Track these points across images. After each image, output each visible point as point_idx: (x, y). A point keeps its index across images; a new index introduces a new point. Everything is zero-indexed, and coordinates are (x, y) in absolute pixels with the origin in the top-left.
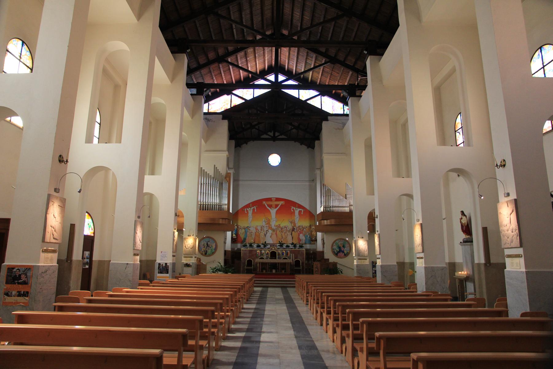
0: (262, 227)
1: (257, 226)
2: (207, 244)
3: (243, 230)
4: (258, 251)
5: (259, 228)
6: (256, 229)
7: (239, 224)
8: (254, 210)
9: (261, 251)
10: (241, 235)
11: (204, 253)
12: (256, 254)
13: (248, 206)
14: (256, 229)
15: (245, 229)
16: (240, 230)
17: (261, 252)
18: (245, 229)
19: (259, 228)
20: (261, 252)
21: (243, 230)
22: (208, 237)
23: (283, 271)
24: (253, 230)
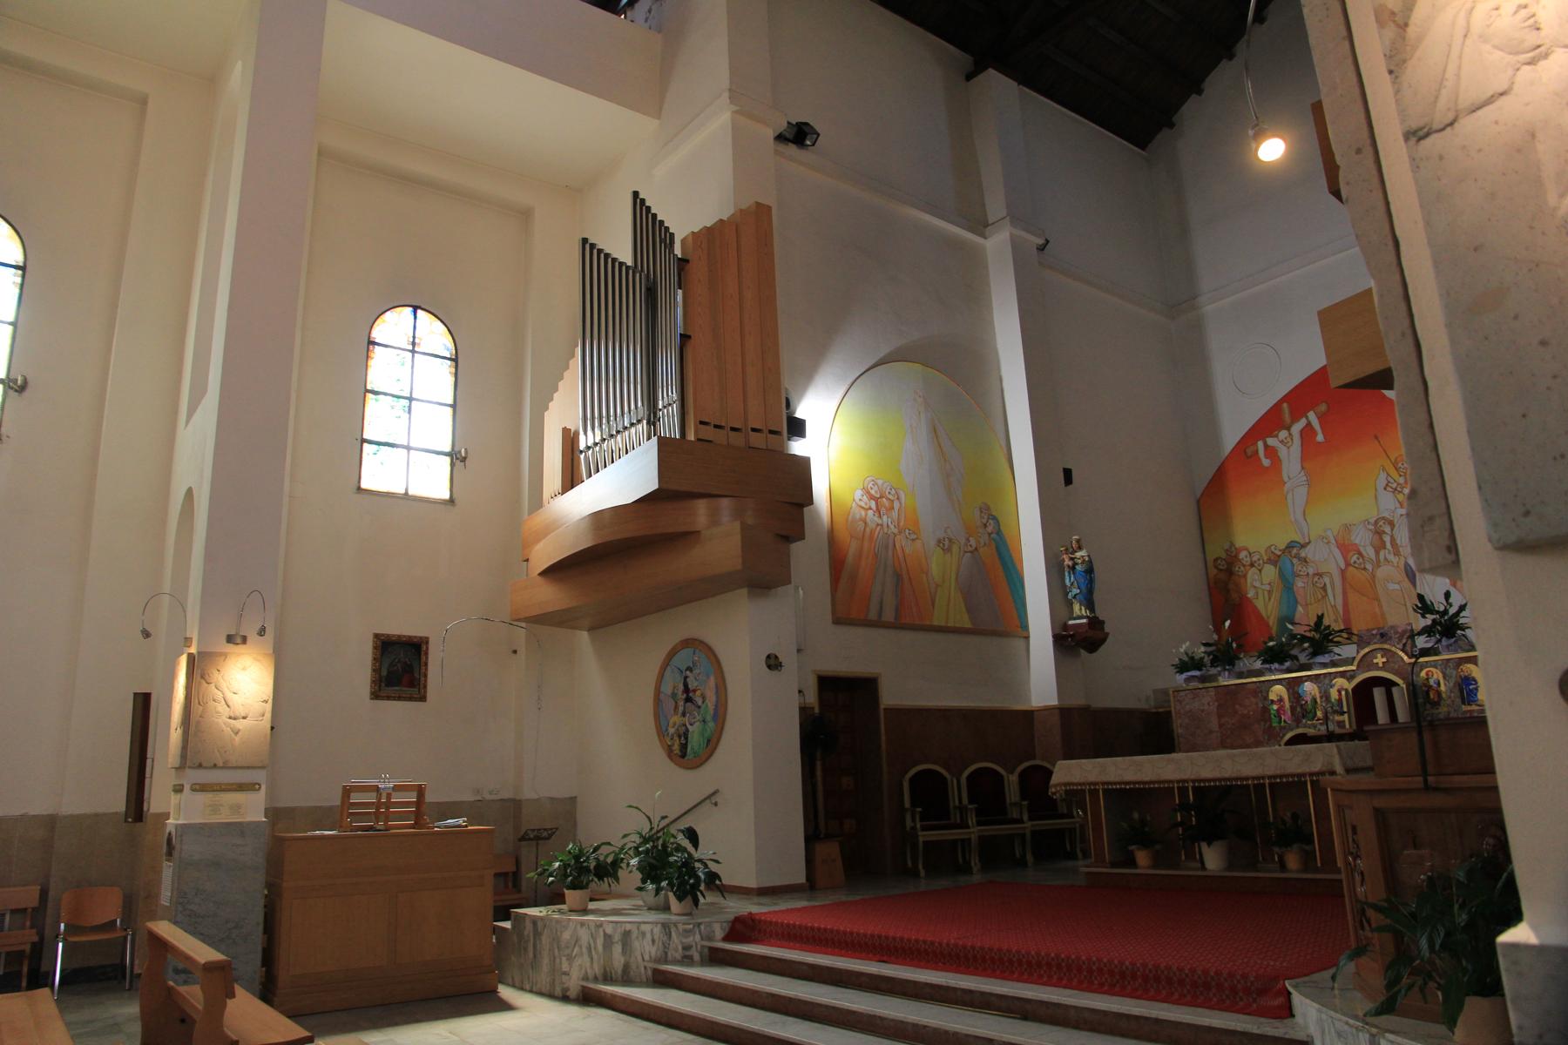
0: (1379, 530)
1: (1347, 528)
2: (686, 690)
3: (1270, 572)
4: (1278, 691)
5: (1362, 538)
6: (1346, 548)
7: (1242, 539)
8: (1308, 432)
9: (1293, 685)
10: (1259, 604)
11: (676, 748)
12: (1266, 710)
13: (1270, 423)
14: (1346, 548)
15: (1274, 560)
16: (1252, 574)
17: (1296, 697)
18: (1274, 560)
19: (1362, 538)
20: (1296, 697)
21: (1270, 572)
22: (687, 643)
23: (1293, 860)
24: (1327, 559)
